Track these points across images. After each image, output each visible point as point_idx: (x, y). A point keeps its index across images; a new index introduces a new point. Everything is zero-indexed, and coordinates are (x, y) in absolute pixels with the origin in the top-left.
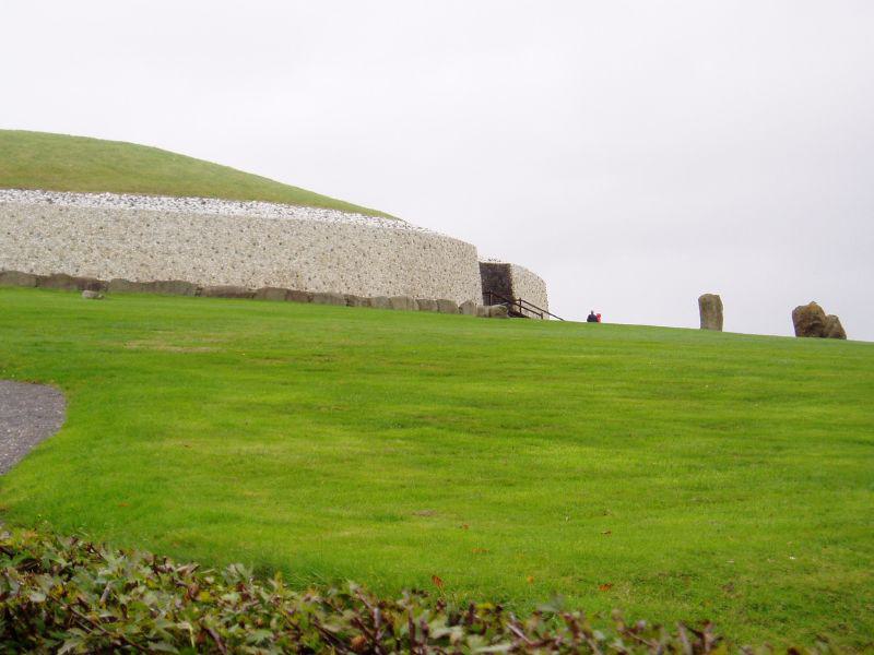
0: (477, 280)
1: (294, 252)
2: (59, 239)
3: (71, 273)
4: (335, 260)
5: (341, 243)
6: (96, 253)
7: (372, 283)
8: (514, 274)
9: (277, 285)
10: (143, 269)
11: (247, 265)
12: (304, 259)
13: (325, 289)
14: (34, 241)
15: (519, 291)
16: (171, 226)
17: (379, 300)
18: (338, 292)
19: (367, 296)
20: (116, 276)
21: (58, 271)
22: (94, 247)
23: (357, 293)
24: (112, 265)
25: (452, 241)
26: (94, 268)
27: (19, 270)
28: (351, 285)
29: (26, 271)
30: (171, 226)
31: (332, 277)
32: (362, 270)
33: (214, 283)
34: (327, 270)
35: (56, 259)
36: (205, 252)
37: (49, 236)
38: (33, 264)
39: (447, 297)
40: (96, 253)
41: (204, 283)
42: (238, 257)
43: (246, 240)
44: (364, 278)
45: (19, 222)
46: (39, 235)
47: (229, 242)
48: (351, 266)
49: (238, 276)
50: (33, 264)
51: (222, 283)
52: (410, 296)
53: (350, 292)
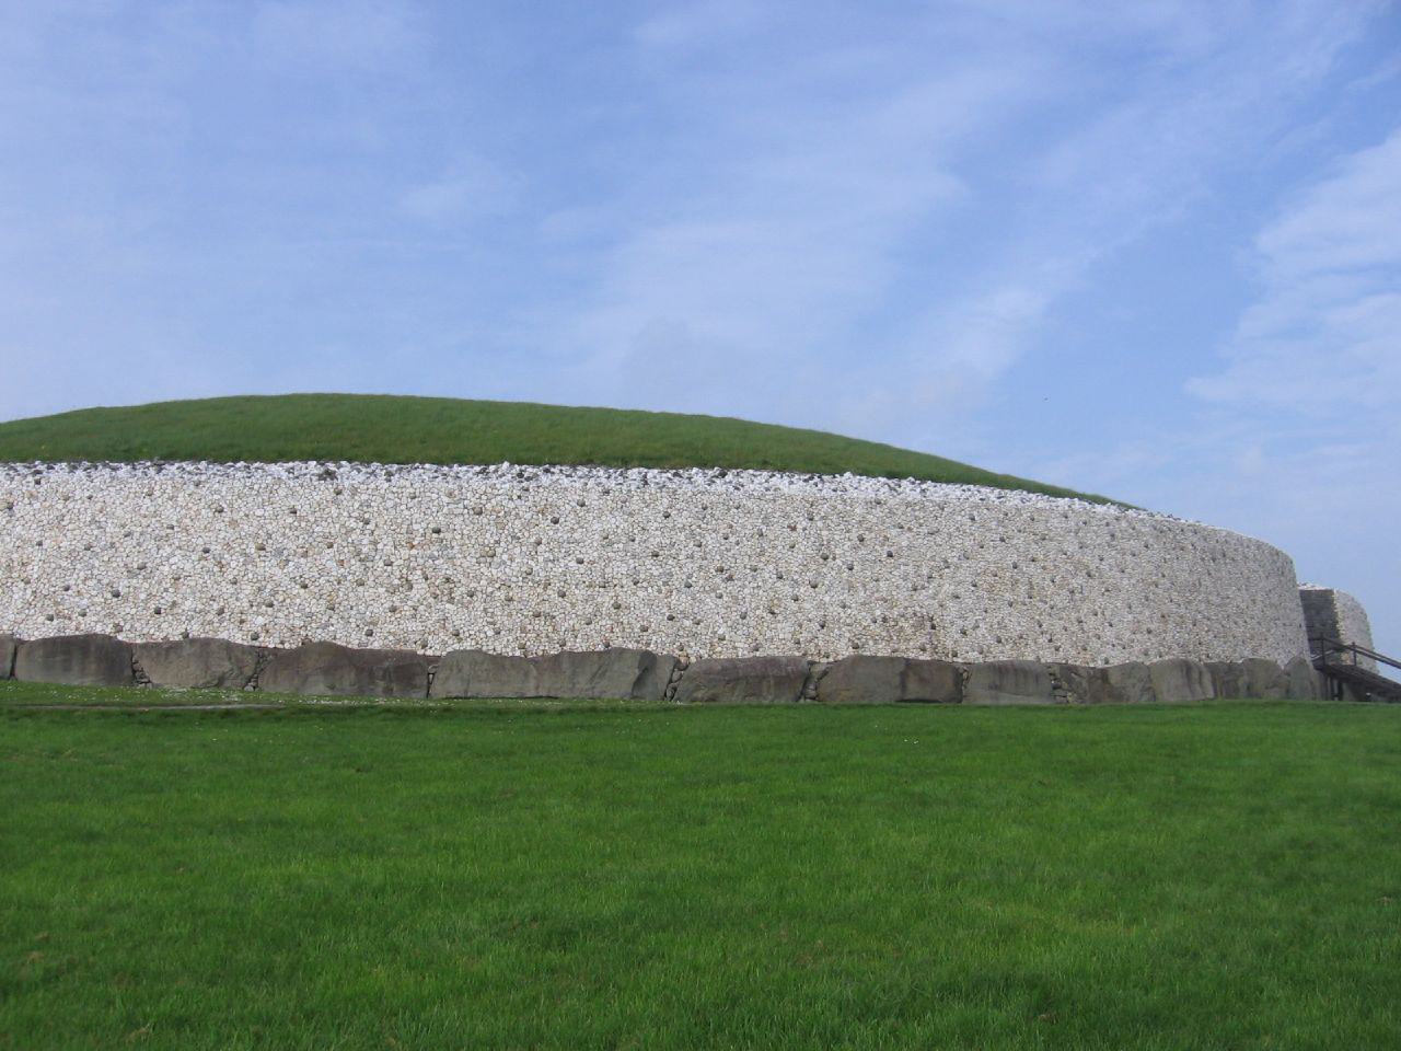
0: (1299, 617)
1: (925, 572)
2: (328, 558)
3: (353, 640)
4: (1023, 589)
5: (1035, 550)
6: (420, 589)
7: (1109, 634)
8: (1339, 606)
9: (883, 651)
10: (539, 624)
11: (807, 606)
12: (948, 588)
13: (1003, 654)
14: (268, 567)
15: (1348, 633)
16: (615, 522)
17: (1129, 669)
18: (1031, 658)
19: (1100, 664)
20: (468, 645)
21: (319, 636)
22: (416, 576)
23: (1076, 659)
24: (458, 616)
25: (1259, 546)
26: (412, 625)
27: (224, 635)
28: (1062, 639)
29: (239, 638)
30: (615, 522)
31: (1015, 625)
32: (1085, 608)
33: (723, 653)
34: (1007, 610)
35: (316, 607)
36: (698, 581)
37: (305, 555)
38: (261, 620)
39: (1262, 654)
40: (420, 589)
41: (696, 651)
42: (785, 589)
43: (805, 548)
44: (1091, 623)
45: (233, 523)
46: (279, 552)
47: (762, 553)
48: (1061, 600)
49: (784, 630)
50: (261, 620)
51: (743, 651)
52: (1192, 658)
53: (1060, 657)
